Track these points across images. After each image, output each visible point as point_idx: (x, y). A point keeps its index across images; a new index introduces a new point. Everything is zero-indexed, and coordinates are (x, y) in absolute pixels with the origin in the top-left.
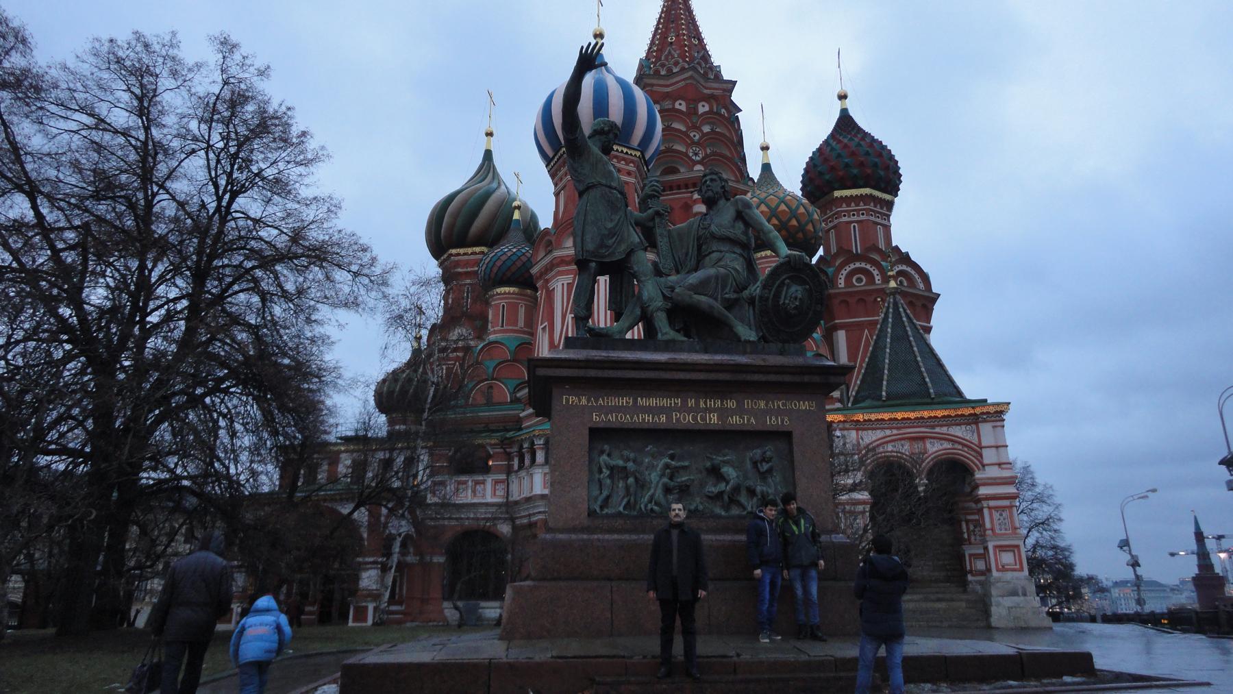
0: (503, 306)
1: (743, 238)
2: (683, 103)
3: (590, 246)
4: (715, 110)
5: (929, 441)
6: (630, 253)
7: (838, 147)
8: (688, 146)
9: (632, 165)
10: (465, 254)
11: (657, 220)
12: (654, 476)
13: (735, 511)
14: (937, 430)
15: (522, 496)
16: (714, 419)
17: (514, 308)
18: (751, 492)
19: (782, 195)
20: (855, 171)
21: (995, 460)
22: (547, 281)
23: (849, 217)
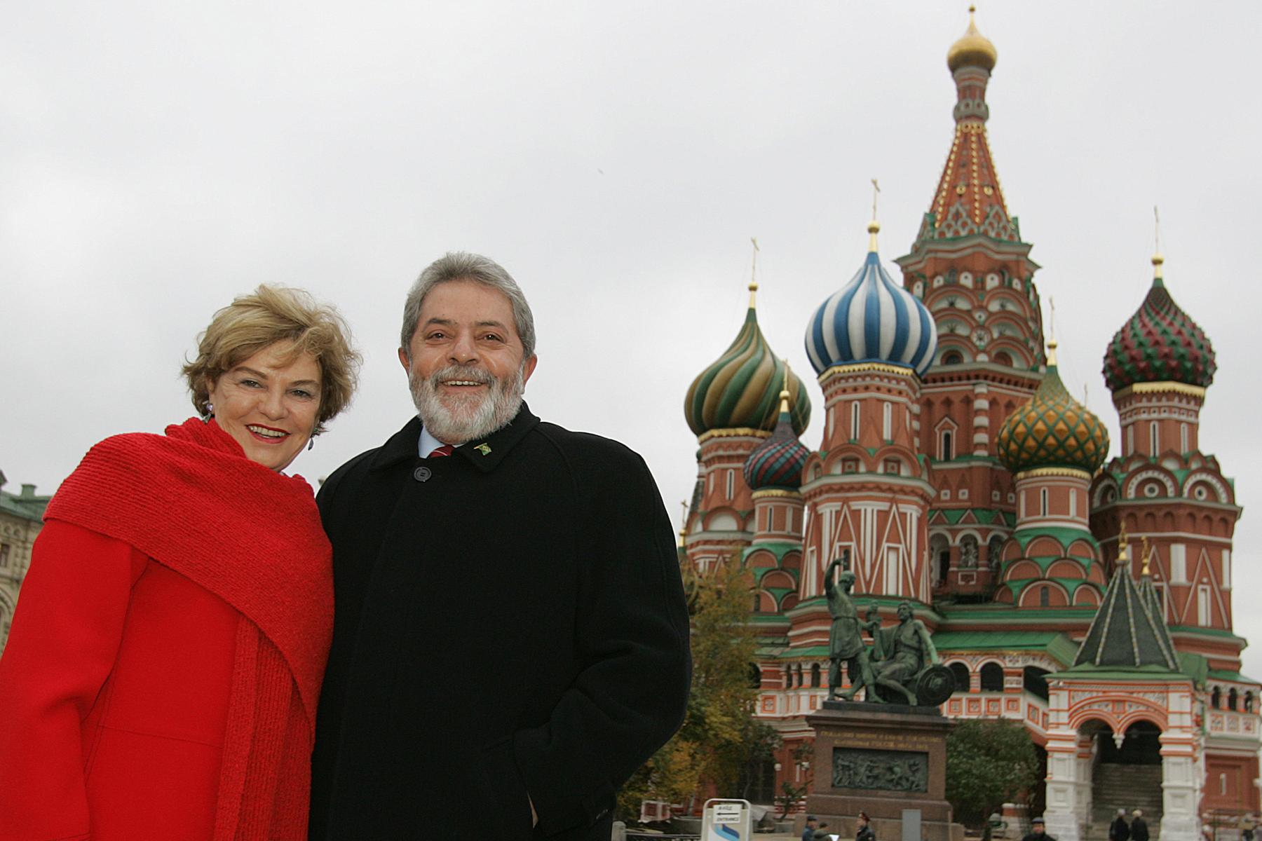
0: (771, 510)
1: (916, 645)
2: (970, 276)
3: (837, 651)
4: (1006, 283)
5: (1127, 704)
6: (857, 655)
7: (1141, 333)
8: (973, 329)
9: (903, 383)
10: (728, 436)
11: (875, 627)
12: (863, 770)
13: (899, 788)
14: (1135, 695)
15: (791, 714)
16: (891, 746)
17: (781, 512)
18: (907, 780)
19: (1061, 410)
20: (1158, 363)
21: (1178, 724)
22: (815, 505)
23: (1149, 413)
